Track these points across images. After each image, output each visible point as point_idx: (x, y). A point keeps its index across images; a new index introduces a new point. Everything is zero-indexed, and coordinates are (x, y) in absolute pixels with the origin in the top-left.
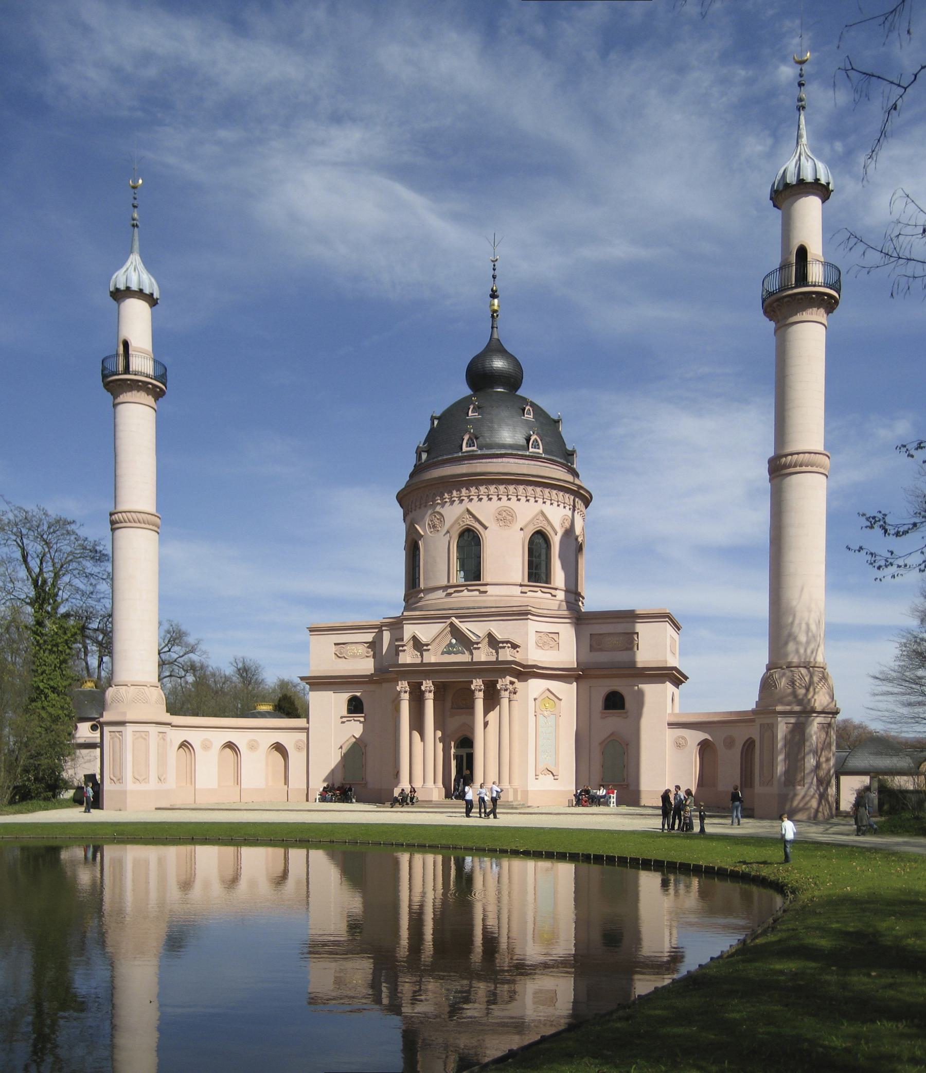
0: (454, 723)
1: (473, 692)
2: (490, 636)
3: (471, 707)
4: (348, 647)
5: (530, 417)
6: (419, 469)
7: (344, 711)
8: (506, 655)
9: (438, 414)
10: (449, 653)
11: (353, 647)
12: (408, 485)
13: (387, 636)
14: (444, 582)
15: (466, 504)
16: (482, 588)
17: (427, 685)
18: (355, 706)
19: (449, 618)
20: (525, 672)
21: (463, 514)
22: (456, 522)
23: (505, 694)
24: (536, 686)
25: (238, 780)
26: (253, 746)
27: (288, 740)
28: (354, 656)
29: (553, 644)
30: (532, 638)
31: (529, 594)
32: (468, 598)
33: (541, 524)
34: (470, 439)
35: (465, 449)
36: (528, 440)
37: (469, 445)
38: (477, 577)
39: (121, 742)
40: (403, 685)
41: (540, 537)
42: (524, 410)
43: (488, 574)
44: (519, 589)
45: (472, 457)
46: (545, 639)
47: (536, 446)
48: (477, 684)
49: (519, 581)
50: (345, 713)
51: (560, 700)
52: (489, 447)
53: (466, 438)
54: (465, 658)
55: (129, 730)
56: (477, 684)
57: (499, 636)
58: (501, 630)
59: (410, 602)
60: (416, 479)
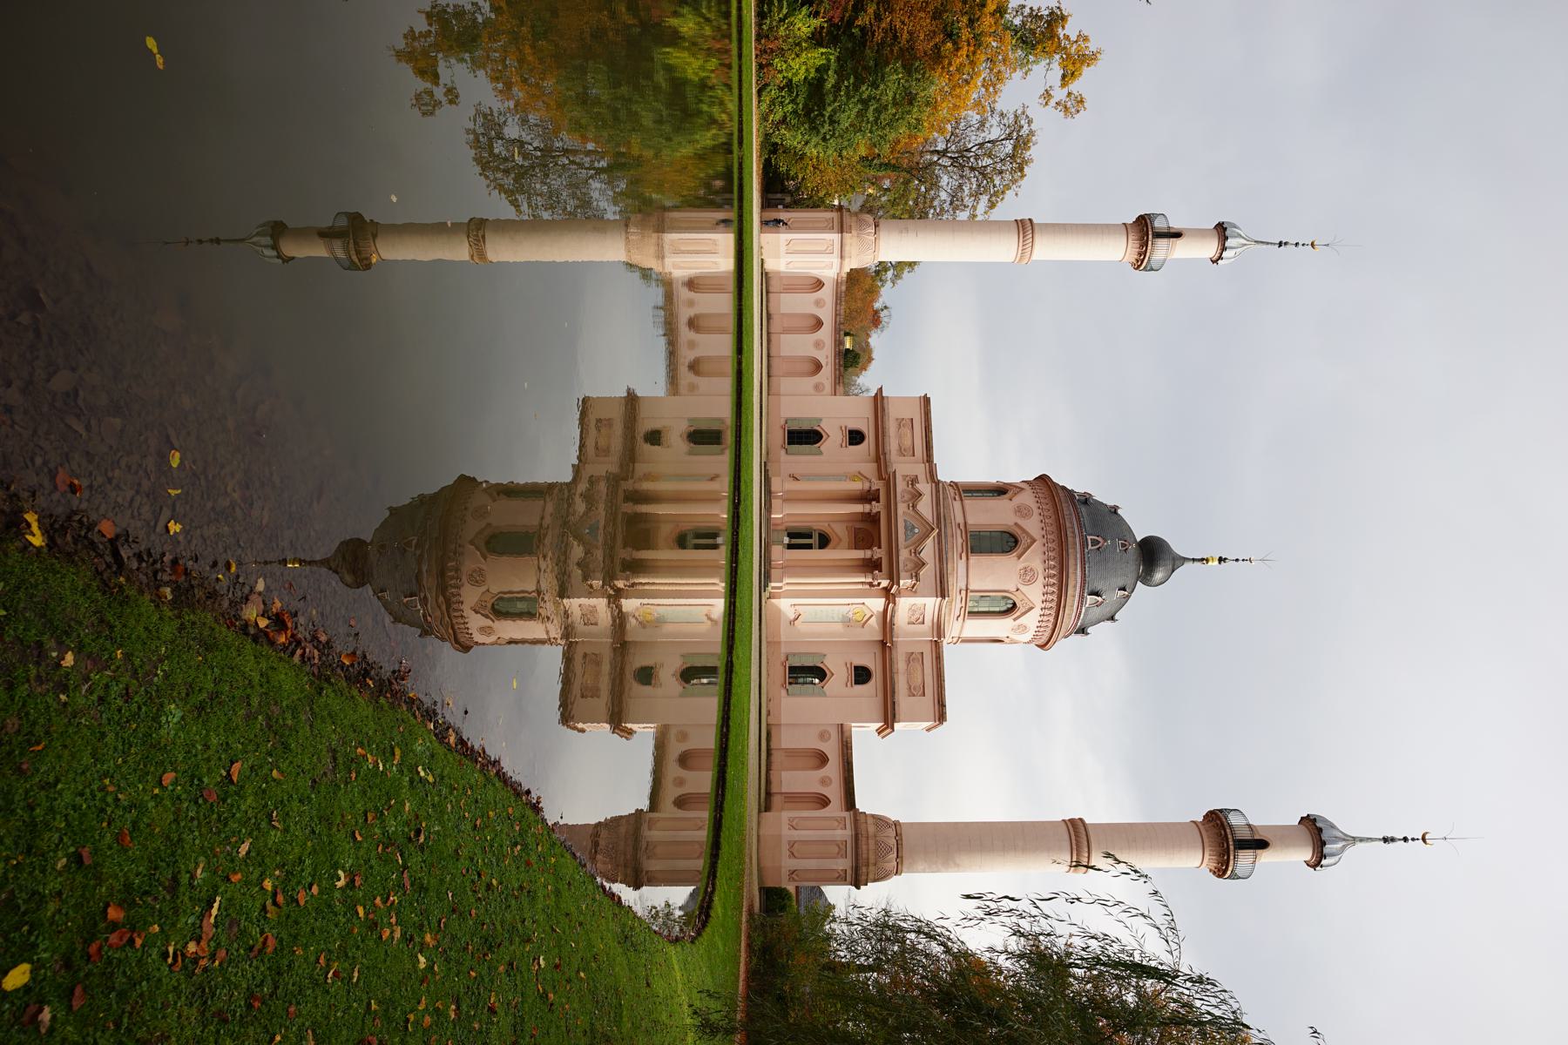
0: (840, 531)
1: (870, 548)
6: (1070, 494)
9: (1119, 511)
10: (906, 528)
11: (909, 435)
12: (1055, 485)
14: (970, 521)
16: (964, 555)
17: (876, 507)
18: (856, 437)
19: (939, 526)
22: (1024, 531)
23: (870, 575)
28: (900, 437)
29: (913, 619)
31: (959, 598)
33: (1021, 608)
34: (1099, 542)
35: (1089, 538)
36: (1097, 594)
41: (1010, 606)
42: (1124, 589)
44: (964, 588)
45: (1084, 544)
48: (879, 553)
51: (863, 626)
53: (1099, 539)
56: (879, 553)
58: (928, 572)
59: (952, 490)
60: (1061, 494)
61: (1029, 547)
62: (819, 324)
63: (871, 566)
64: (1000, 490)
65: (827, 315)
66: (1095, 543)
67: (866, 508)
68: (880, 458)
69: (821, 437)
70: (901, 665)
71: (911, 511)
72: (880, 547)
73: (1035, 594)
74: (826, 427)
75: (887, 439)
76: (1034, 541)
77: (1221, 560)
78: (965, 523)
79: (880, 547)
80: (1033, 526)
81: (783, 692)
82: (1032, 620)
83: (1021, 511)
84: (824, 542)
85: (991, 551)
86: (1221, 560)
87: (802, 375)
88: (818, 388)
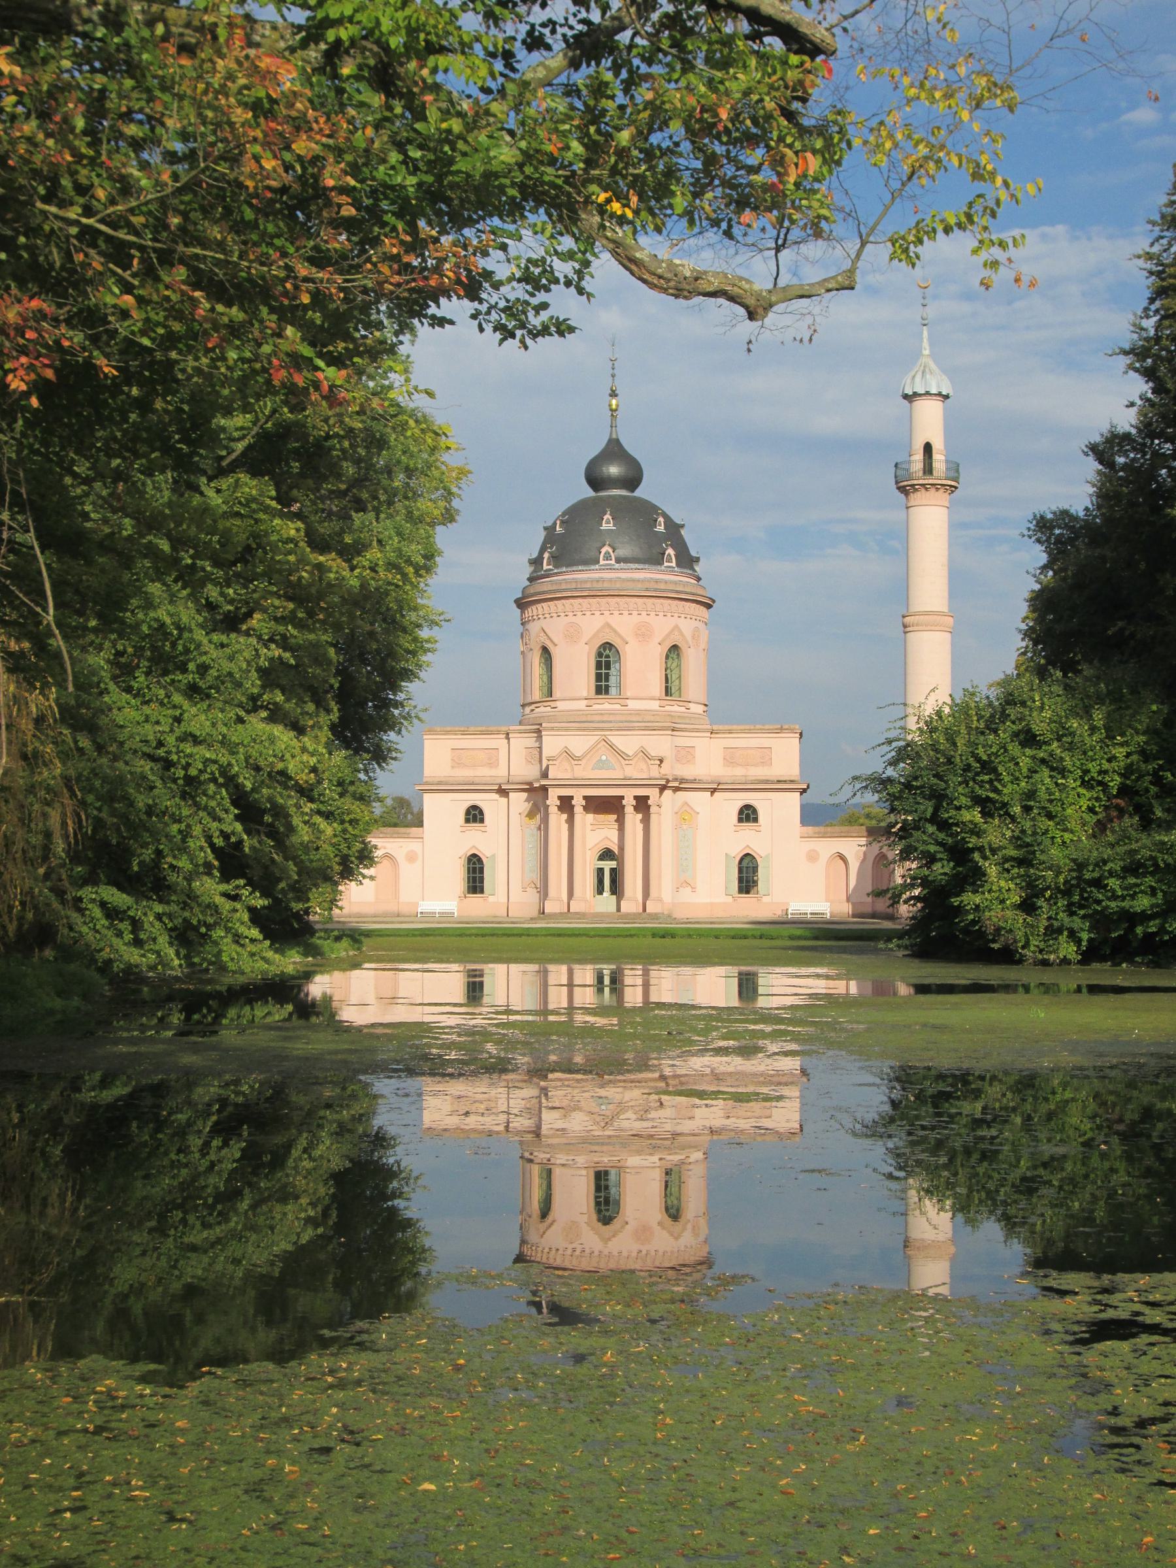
5: (661, 528)
14: (585, 694)
15: (607, 617)
18: (474, 815)
21: (603, 627)
22: (595, 635)
34: (607, 553)
37: (608, 558)
47: (670, 561)
53: (603, 550)
61: (615, 631)
63: (642, 804)
66: (608, 557)
67: (578, 809)
69: (474, 855)
70: (738, 772)
71: (583, 762)
72: (622, 797)
74: (466, 850)
75: (477, 780)
76: (608, 625)
79: (622, 797)
81: (765, 899)
83: (572, 635)
86: (614, 394)
87: (396, 877)
88: (411, 857)
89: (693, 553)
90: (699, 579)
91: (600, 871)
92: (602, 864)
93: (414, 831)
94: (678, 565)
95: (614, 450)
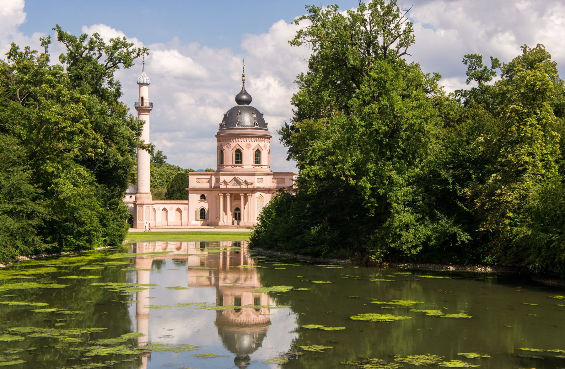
0: (235, 204)
1: (240, 196)
2: (245, 181)
3: (240, 199)
4: (201, 180)
5: (255, 116)
7: (199, 199)
8: (250, 187)
13: (214, 178)
14: (232, 164)
18: (203, 197)
20: (254, 191)
24: (257, 194)
25: (167, 219)
26: (171, 209)
27: (182, 207)
28: (203, 182)
30: (256, 180)
32: (238, 169)
33: (258, 147)
37: (238, 125)
38: (241, 163)
39: (142, 209)
40: (221, 194)
43: (244, 163)
44: (252, 166)
46: (260, 180)
48: (242, 195)
49: (252, 164)
50: (200, 199)
52: (244, 126)
54: (238, 187)
55: (145, 206)
56: (242, 195)
57: (248, 181)
58: (249, 179)
62: (165, 209)
64: (221, 154)
65: (162, 207)
68: (210, 190)
69: (203, 209)
73: (254, 144)
77: (243, 76)
78: (232, 165)
80: (234, 144)
82: (262, 144)
84: (238, 209)
85: (241, 159)
88: (185, 210)
89: (266, 122)
90: (267, 130)
91: (236, 214)
92: (236, 212)
93: (186, 202)
94: (259, 127)
95: (244, 92)
